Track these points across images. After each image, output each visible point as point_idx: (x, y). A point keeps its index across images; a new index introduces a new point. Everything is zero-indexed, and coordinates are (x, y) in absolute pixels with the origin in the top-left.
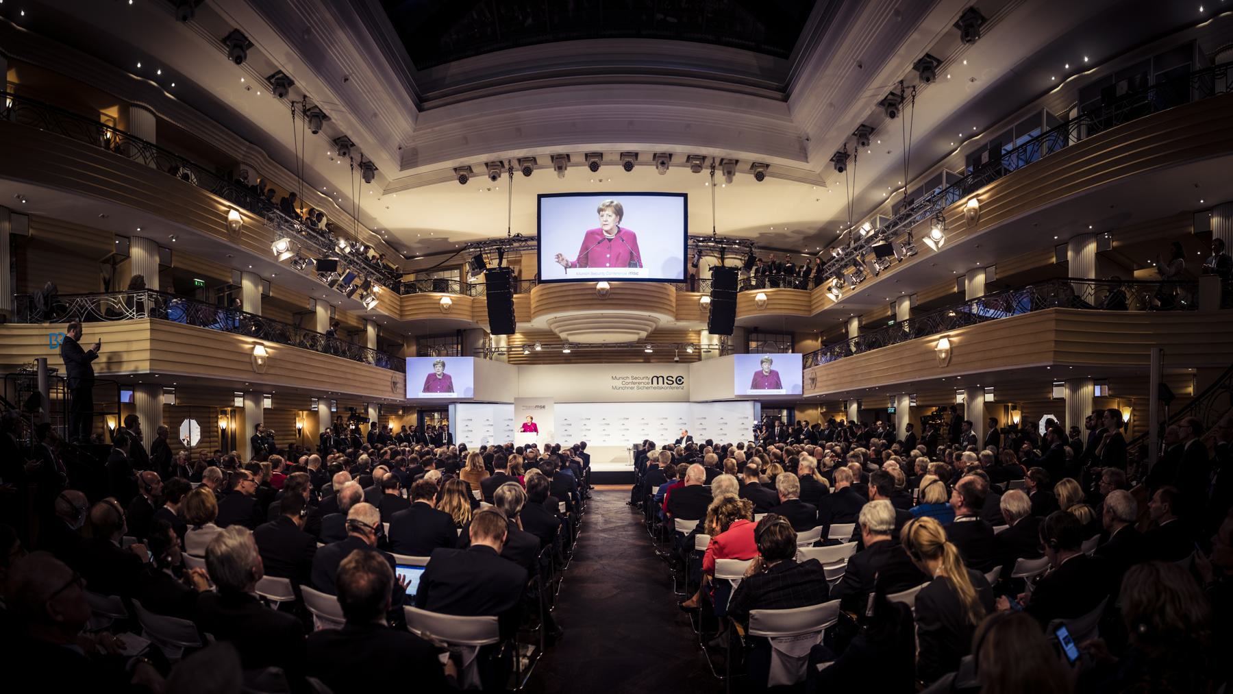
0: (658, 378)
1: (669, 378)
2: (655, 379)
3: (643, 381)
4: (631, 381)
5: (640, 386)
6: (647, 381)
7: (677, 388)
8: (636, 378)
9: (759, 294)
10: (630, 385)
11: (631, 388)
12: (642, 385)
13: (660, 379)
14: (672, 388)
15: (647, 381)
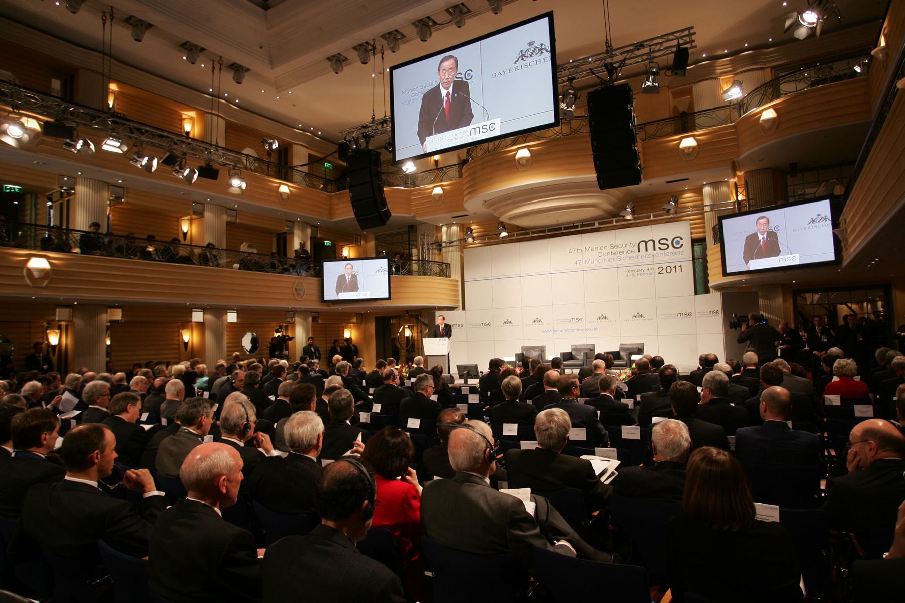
0: (646, 243)
2: (642, 245)
5: (622, 256)
8: (616, 247)
9: (764, 113)
10: (609, 257)
12: (625, 255)
13: (650, 244)
15: (631, 249)
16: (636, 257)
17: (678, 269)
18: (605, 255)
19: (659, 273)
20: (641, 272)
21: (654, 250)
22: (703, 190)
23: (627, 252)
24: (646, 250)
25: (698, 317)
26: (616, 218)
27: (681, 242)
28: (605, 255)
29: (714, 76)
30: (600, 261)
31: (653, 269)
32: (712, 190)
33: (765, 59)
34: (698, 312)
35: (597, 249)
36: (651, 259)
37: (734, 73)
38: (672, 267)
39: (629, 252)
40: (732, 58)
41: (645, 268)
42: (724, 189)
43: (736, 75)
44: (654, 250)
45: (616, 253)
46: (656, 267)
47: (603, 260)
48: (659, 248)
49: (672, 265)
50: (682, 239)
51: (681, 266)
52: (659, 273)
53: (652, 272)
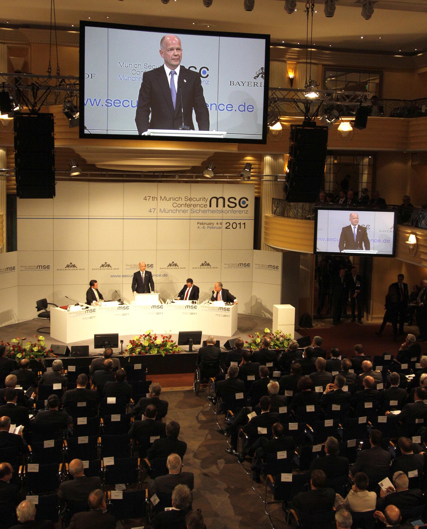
0: (217, 199)
1: (232, 200)
2: (214, 201)
3: (200, 203)
4: (184, 202)
6: (204, 203)
7: (240, 212)
8: (190, 199)
10: (183, 208)
11: (183, 212)
12: (198, 208)
13: (221, 201)
14: (234, 212)
15: (204, 203)
16: (208, 211)
17: (242, 226)
18: (179, 206)
19: (226, 228)
20: (211, 226)
21: (224, 206)
22: (265, 158)
23: (200, 206)
24: (217, 206)
25: (256, 268)
26: (196, 174)
27: (247, 203)
28: (179, 206)
29: (284, 59)
30: (174, 211)
31: (221, 224)
32: (272, 159)
33: (320, 57)
34: (256, 264)
35: (172, 199)
36: (221, 215)
37: (298, 61)
38: (237, 224)
39: (202, 206)
40: (301, 49)
41: (215, 222)
42: (281, 160)
43: (299, 63)
44: (224, 206)
45: (190, 205)
46: (224, 222)
47: (177, 211)
48: (228, 206)
49: (238, 222)
50: (247, 200)
51: (244, 224)
52: (226, 228)
53: (221, 226)
